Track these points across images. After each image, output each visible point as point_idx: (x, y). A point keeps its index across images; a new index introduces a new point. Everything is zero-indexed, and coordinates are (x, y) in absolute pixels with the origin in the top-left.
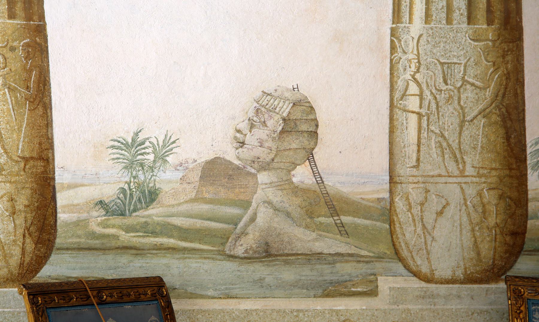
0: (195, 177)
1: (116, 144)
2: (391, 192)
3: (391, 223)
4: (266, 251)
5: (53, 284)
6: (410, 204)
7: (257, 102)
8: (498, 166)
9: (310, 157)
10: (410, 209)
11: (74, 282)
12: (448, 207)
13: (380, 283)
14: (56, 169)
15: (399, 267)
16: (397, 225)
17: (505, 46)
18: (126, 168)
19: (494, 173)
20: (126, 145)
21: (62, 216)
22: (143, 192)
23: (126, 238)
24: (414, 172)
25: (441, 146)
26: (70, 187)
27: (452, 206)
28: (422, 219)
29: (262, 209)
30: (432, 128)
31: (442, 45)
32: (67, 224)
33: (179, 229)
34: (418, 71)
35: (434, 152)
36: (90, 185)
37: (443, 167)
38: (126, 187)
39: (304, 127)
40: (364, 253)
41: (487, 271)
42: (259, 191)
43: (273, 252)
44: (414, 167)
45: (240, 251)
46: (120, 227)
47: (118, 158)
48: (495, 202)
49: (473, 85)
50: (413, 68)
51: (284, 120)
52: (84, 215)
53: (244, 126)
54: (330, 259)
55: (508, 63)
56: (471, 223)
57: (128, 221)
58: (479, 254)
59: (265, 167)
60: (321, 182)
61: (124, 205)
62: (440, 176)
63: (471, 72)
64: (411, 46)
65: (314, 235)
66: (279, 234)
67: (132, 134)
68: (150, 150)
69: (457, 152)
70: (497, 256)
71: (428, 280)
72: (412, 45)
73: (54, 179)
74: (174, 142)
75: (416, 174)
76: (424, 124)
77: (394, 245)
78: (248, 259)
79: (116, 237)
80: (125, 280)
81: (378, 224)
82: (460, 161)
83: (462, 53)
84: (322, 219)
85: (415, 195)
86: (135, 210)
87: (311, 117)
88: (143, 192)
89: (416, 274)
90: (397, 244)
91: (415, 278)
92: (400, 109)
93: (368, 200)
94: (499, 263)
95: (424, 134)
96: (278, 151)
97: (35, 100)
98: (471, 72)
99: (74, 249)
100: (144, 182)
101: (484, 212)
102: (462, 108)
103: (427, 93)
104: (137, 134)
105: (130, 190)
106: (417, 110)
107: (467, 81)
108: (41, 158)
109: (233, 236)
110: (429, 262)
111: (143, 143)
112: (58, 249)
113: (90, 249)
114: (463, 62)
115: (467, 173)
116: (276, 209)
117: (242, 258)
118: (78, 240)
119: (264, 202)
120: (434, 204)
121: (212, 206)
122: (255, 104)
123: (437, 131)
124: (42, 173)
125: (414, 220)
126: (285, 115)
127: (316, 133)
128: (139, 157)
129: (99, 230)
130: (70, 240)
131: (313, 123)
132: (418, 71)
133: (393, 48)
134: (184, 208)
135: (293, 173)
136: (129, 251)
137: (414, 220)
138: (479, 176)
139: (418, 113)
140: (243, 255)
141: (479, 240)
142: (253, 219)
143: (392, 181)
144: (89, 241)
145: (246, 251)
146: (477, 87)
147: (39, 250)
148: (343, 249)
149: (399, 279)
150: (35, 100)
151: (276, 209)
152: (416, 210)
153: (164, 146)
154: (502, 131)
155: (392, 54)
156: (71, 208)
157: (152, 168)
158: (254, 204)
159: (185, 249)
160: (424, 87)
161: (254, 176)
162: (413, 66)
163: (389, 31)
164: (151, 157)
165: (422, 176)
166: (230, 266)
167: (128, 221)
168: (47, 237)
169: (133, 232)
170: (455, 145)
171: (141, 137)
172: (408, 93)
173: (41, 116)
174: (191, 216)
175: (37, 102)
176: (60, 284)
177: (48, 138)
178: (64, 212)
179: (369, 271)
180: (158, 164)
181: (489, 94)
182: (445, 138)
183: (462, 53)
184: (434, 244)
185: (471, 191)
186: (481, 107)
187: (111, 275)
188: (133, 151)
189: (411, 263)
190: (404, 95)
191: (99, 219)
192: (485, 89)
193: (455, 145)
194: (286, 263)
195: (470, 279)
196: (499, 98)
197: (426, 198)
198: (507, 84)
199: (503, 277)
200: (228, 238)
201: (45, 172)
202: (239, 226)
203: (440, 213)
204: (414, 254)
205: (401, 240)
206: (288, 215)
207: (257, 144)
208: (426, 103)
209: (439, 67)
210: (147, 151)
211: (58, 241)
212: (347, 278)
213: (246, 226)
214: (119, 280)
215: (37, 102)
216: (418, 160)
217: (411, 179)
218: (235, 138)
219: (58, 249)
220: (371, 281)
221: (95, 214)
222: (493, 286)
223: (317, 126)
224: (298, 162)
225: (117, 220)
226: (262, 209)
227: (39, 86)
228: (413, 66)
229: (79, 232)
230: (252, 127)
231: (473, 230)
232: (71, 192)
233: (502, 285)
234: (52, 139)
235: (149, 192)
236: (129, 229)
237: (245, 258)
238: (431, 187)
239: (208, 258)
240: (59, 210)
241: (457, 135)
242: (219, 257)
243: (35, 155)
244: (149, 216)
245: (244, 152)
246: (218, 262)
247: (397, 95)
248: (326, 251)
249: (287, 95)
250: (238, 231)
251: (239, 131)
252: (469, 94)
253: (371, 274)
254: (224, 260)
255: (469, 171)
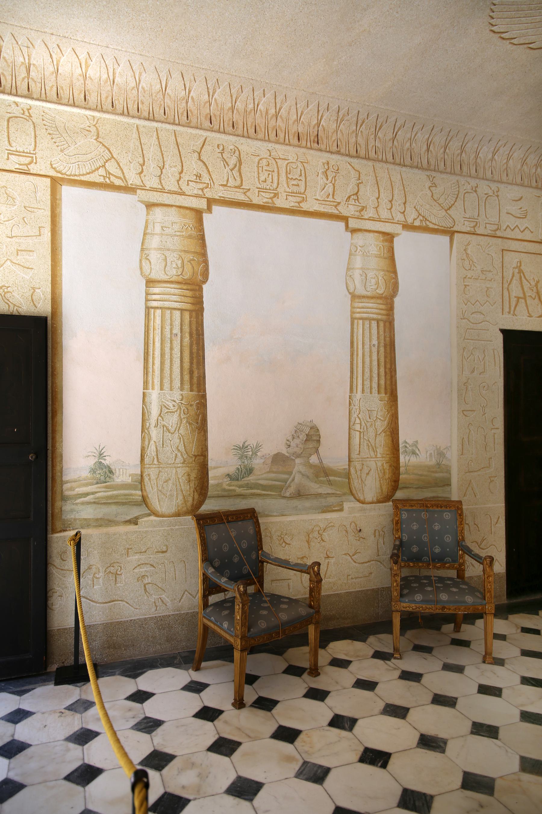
0: (269, 461)
1: (235, 447)
2: (349, 465)
3: (349, 479)
4: (299, 494)
5: (207, 514)
6: (356, 471)
7: (296, 428)
8: (389, 453)
9: (317, 451)
10: (356, 473)
11: (217, 513)
12: (371, 471)
13: (344, 505)
14: (209, 460)
15: (352, 498)
16: (351, 480)
17: (391, 403)
18: (239, 458)
19: (388, 456)
20: (240, 448)
21: (211, 482)
22: (247, 469)
23: (239, 490)
24: (358, 456)
25: (368, 445)
26: (215, 468)
27: (372, 470)
28: (361, 477)
29: (297, 475)
30: (365, 437)
31: (368, 402)
32: (213, 485)
33: (262, 485)
34: (359, 413)
35: (366, 447)
36: (224, 467)
37: (369, 454)
38: (239, 467)
39: (315, 438)
40: (338, 492)
41: (385, 497)
42: (296, 467)
43: (302, 494)
44: (358, 454)
45: (288, 494)
46: (236, 486)
47: (236, 454)
48: (388, 468)
49: (380, 419)
50: (358, 412)
51: (307, 435)
52: (221, 481)
53: (290, 438)
54: (325, 496)
55: (392, 410)
56: (379, 478)
57: (240, 483)
58: (382, 491)
59: (299, 456)
60: (321, 462)
61: (238, 476)
62: (368, 458)
63: (379, 414)
64: (357, 403)
65: (318, 486)
66: (304, 486)
67: (242, 443)
68: (250, 450)
69: (374, 447)
70: (389, 492)
71: (363, 502)
72: (357, 402)
73: (208, 465)
74: (260, 446)
75: (359, 457)
76: (362, 436)
77: (350, 488)
78: (291, 498)
79: (234, 490)
80: (238, 511)
81: (344, 479)
82: (375, 451)
83: (376, 406)
84: (322, 479)
85: (358, 467)
86: (243, 478)
87: (318, 433)
88: (247, 469)
89: (359, 501)
90: (351, 488)
91: (358, 502)
92: (353, 430)
93: (340, 469)
94: (390, 494)
95: (362, 440)
96: (304, 449)
97: (200, 428)
98: (379, 414)
99: (216, 497)
100: (247, 465)
101: (384, 473)
102: (376, 429)
103: (363, 422)
104: (244, 443)
105: (241, 468)
106: (359, 430)
107: (378, 418)
108: (202, 455)
109: (285, 488)
110: (364, 495)
111: (247, 447)
112: (209, 497)
113: (223, 496)
114: (376, 410)
115: (378, 457)
116: (303, 475)
117: (288, 498)
118: (218, 493)
119: (298, 472)
120: (366, 470)
121: (276, 474)
122: (295, 428)
123: (367, 439)
124: (203, 462)
125: (358, 477)
126: (307, 433)
127: (320, 440)
128: (245, 453)
129: (227, 487)
130: (214, 493)
131: (318, 436)
132: (359, 413)
133: (350, 404)
134: (264, 476)
135: (310, 458)
136: (240, 497)
137: (358, 477)
138: (382, 457)
139: (359, 431)
140: (288, 496)
141: (382, 485)
142: (293, 480)
143: (350, 461)
144: (223, 493)
145: (290, 494)
146: (381, 420)
147: (200, 498)
148: (330, 491)
149: (352, 503)
150: (200, 428)
151: (303, 475)
152: (359, 473)
153: (256, 448)
154: (391, 438)
155: (349, 406)
156: (215, 478)
157: (251, 458)
158: (294, 473)
159: (264, 495)
160: (362, 420)
161: (294, 460)
162: (358, 411)
163: (348, 397)
164: (251, 453)
165: (361, 458)
166: (283, 501)
167: (240, 483)
168: (204, 492)
169: (242, 488)
170: (373, 445)
171: (246, 444)
172: (356, 423)
173: (203, 436)
174: (267, 479)
175: (201, 429)
176: (210, 514)
177: (206, 446)
178: (212, 480)
179: (340, 500)
180: (253, 456)
181: (386, 423)
182: (370, 442)
183: (376, 406)
184: (365, 487)
185: (379, 464)
186: (383, 428)
187: (233, 508)
188: (243, 450)
189: (356, 495)
190: (354, 423)
191: (227, 482)
192: (384, 421)
193: (373, 445)
194: (307, 498)
195: (379, 502)
196: (390, 425)
197: (362, 468)
198: (392, 419)
199: (391, 500)
200: (283, 489)
201: (204, 462)
202: (287, 483)
203: (368, 474)
204: (358, 492)
205: (353, 486)
206: (308, 477)
207: (295, 446)
208: (362, 427)
209: (367, 412)
210: (249, 450)
211: (209, 493)
212: (331, 504)
213: (291, 483)
214: (236, 511)
215: (201, 429)
216: (359, 451)
217: (357, 460)
218: (286, 444)
219: (209, 497)
220: (341, 505)
221: (225, 480)
222: (387, 504)
223: (320, 437)
224: (312, 454)
225: (235, 483)
226: (297, 475)
227: (202, 422)
228: (358, 411)
229: (219, 489)
230: (293, 438)
231: (380, 480)
232: (215, 471)
233: (391, 503)
234: (207, 446)
235: (249, 469)
236: (240, 487)
237: (290, 497)
238: (364, 463)
239: (274, 498)
240: (210, 479)
241: (374, 440)
242: (279, 497)
243: (199, 454)
244: (249, 480)
245: (291, 450)
246: (279, 500)
247: (352, 424)
248: (323, 493)
249: (308, 424)
250: (287, 485)
251: (288, 440)
252: (378, 423)
253: (341, 502)
254: (281, 498)
255: (379, 455)
